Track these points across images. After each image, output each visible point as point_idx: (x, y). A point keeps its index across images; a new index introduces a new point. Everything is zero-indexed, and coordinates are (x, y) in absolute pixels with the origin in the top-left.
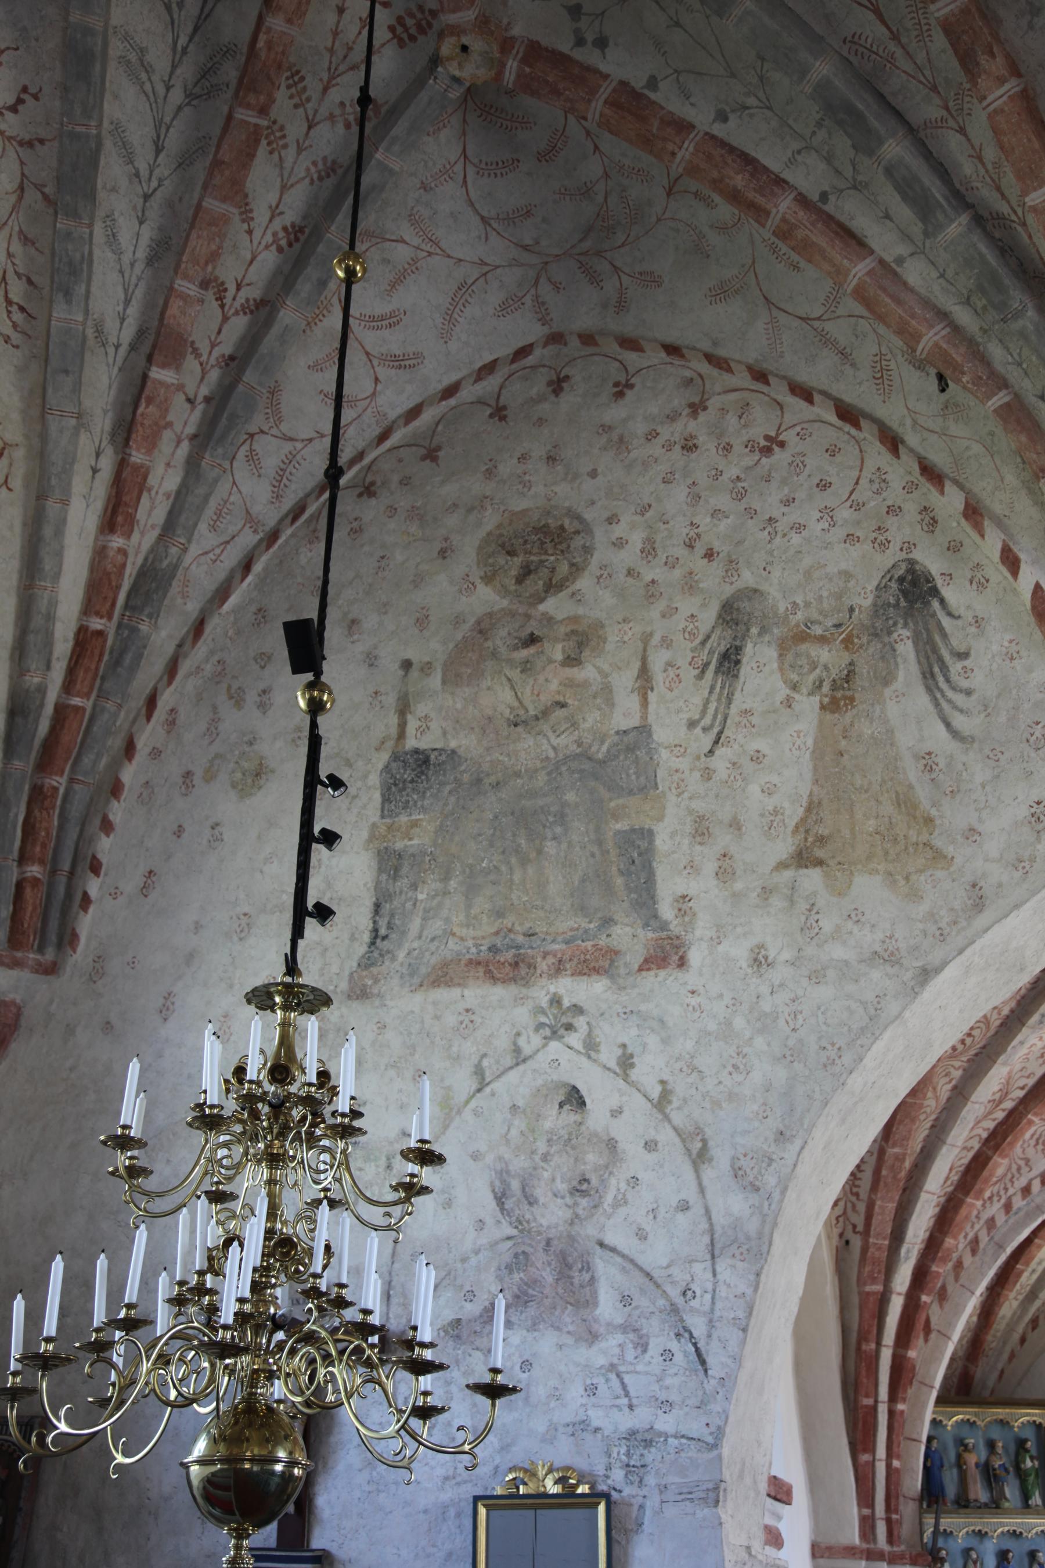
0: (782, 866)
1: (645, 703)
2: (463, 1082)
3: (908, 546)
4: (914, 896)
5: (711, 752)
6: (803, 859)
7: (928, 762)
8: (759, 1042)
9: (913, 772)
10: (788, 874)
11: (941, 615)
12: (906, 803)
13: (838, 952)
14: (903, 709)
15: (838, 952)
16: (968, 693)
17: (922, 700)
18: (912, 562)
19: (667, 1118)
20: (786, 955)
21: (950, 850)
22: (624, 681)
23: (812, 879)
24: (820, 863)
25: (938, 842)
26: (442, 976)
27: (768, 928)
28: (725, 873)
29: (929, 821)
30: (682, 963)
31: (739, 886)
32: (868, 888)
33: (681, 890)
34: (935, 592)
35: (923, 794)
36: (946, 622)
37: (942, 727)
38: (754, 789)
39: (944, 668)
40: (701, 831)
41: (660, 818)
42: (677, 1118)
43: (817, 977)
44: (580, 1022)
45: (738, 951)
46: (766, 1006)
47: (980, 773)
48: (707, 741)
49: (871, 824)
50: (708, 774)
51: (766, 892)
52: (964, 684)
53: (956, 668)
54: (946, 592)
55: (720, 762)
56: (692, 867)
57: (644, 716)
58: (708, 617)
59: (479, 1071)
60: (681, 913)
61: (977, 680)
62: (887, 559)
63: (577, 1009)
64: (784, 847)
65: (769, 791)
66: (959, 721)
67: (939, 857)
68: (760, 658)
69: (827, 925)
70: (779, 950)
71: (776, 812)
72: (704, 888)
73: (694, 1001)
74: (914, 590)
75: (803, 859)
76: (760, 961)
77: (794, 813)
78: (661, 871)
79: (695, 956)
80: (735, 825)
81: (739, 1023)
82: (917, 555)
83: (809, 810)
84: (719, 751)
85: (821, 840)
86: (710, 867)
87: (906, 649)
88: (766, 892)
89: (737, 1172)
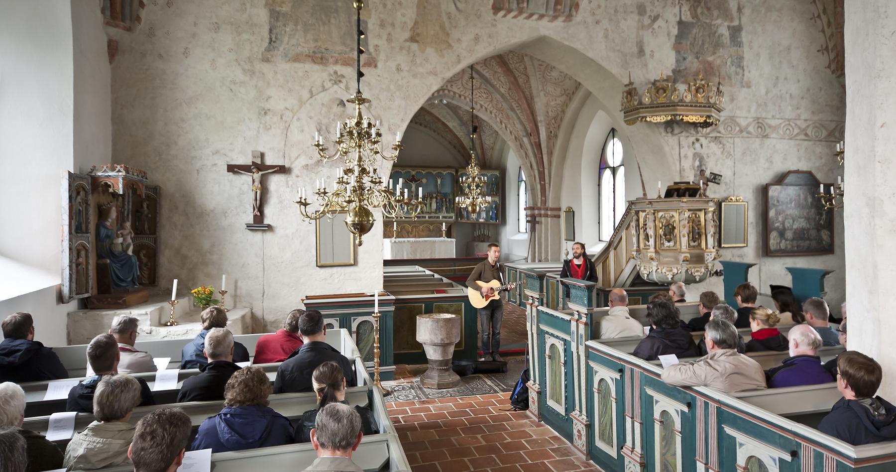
0: (406, 41)
2: (305, 94)
4: (442, 56)
6: (413, 39)
7: (449, 15)
8: (398, 93)
9: (445, 18)
10: (408, 44)
12: (442, 27)
13: (421, 70)
15: (421, 70)
20: (407, 69)
21: (453, 44)
23: (415, 46)
24: (417, 42)
25: (450, 41)
26: (297, 59)
27: (402, 59)
28: (389, 40)
29: (448, 34)
30: (376, 66)
31: (393, 45)
32: (430, 51)
33: (376, 43)
35: (447, 25)
37: (453, 6)
38: (399, 14)
40: (382, 25)
41: (370, 18)
42: (373, 112)
43: (415, 76)
44: (344, 80)
45: (393, 65)
46: (400, 82)
47: (463, 22)
49: (432, 32)
51: (402, 48)
56: (379, 36)
59: (311, 92)
60: (376, 50)
63: (343, 76)
64: (407, 35)
65: (403, 15)
66: (458, 4)
67: (450, 46)
69: (418, 61)
70: (404, 66)
71: (405, 23)
72: (382, 43)
73: (379, 78)
75: (413, 39)
76: (399, 69)
77: (410, 24)
79: (380, 65)
80: (393, 25)
81: (392, 87)
83: (415, 24)
85: (418, 35)
86: (385, 37)
88: (402, 48)
89: (389, 129)
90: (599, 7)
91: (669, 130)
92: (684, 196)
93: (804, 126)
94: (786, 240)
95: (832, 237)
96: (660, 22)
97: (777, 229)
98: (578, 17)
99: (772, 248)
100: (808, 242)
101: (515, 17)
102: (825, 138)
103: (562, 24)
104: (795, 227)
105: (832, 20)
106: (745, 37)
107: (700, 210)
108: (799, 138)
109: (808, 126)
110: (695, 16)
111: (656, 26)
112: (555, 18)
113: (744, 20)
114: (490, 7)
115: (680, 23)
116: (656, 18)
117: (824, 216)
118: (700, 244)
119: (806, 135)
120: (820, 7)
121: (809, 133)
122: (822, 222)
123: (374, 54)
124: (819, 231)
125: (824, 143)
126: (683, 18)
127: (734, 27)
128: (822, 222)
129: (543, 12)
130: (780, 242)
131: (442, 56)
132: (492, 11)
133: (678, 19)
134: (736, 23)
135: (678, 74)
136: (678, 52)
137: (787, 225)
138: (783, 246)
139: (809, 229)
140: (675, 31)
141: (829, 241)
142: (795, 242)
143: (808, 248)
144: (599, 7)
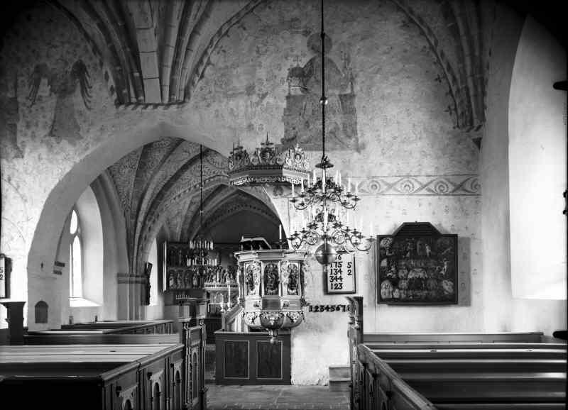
0: (45, 136)
1: (16, 91)
3: (80, 57)
5: (31, 106)
10: (47, 138)
11: (86, 76)
14: (77, 98)
16: (91, 97)
17: (80, 95)
18: (81, 61)
19: (18, 193)
22: (11, 85)
30: (23, 157)
34: (85, 69)
36: (88, 78)
39: (86, 91)
40: (28, 126)
48: (31, 103)
50: (31, 111)
51: (42, 141)
52: (90, 94)
53: (88, 90)
54: (89, 70)
55: (33, 109)
57: (16, 95)
58: (32, 69)
60: (23, 146)
61: (93, 94)
62: (76, 60)
64: (48, 130)
68: (45, 81)
74: (80, 70)
75: (51, 134)
76: (40, 159)
77: (50, 123)
78: (19, 135)
82: (83, 59)
84: (34, 106)
87: (79, 84)
88: (42, 141)
90: (210, 92)
91: (278, 192)
92: (249, 249)
93: (425, 180)
94: (400, 289)
95: (455, 287)
96: (269, 99)
97: (389, 278)
98: (191, 103)
99: (383, 297)
100: (426, 292)
101: (133, 109)
102: (454, 191)
103: (176, 110)
104: (410, 277)
105: (458, 76)
106: (357, 103)
107: (277, 261)
108: (420, 193)
109: (431, 182)
110: (305, 90)
111: (264, 102)
112: (169, 105)
113: (357, 88)
114: (113, 103)
115: (288, 97)
116: (264, 96)
117: (445, 267)
118: (277, 293)
119: (429, 190)
120: (445, 66)
121: (433, 189)
122: (443, 272)
123: (22, 150)
124: (439, 281)
125: (451, 197)
126: (293, 93)
127: (345, 95)
128: (443, 272)
129: (159, 101)
130: (394, 291)
131: (74, 145)
132: (115, 107)
133: (287, 94)
134: (348, 91)
135: (289, 142)
136: (287, 124)
137: (401, 274)
138: (396, 295)
139: (426, 279)
140: (284, 105)
141: (451, 291)
142: (410, 293)
143: (426, 298)
144: (210, 92)
